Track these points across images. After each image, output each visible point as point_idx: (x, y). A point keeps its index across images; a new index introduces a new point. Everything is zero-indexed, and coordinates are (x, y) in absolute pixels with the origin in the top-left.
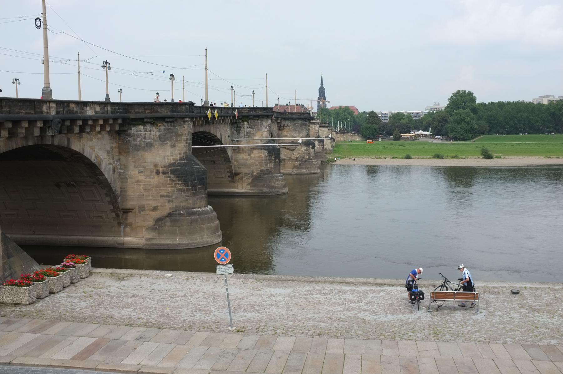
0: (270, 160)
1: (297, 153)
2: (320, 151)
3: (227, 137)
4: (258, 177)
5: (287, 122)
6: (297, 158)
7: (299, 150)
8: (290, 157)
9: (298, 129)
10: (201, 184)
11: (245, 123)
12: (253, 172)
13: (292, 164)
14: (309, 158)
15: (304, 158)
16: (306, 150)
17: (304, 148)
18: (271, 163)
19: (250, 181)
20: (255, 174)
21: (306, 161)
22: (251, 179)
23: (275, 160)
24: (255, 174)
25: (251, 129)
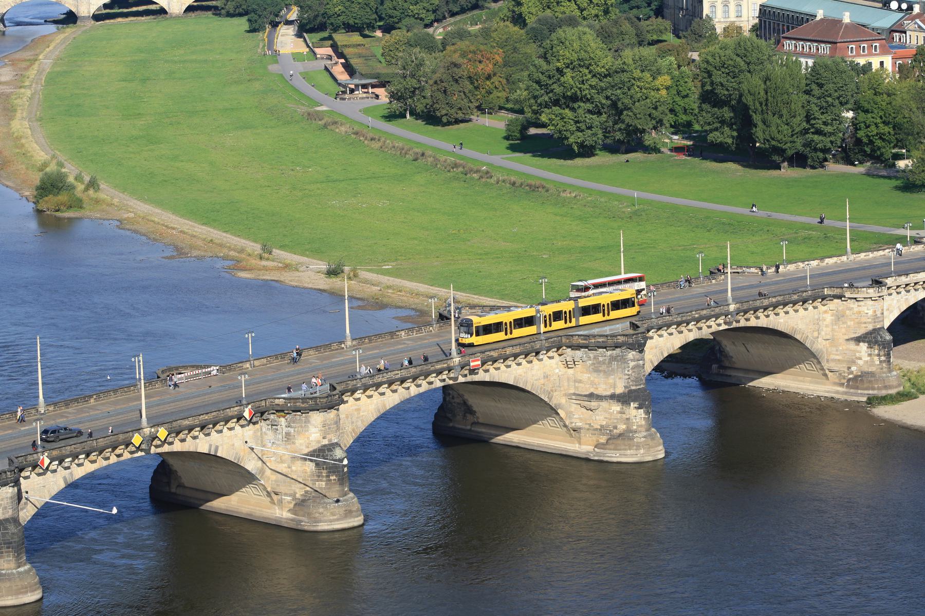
0: (319, 476)
1: (602, 417)
2: (873, 369)
3: (238, 444)
4: (303, 501)
5: (579, 353)
6: (602, 426)
7: (605, 411)
8: (590, 424)
9: (603, 367)
10: (8, 548)
11: (283, 420)
12: (295, 493)
13: (594, 438)
14: (628, 430)
15: (615, 428)
16: (622, 412)
17: (616, 407)
18: (322, 481)
19: (292, 506)
20: (298, 496)
21: (620, 435)
22: (294, 503)
23: (328, 476)
24: (298, 496)
25: (292, 430)
